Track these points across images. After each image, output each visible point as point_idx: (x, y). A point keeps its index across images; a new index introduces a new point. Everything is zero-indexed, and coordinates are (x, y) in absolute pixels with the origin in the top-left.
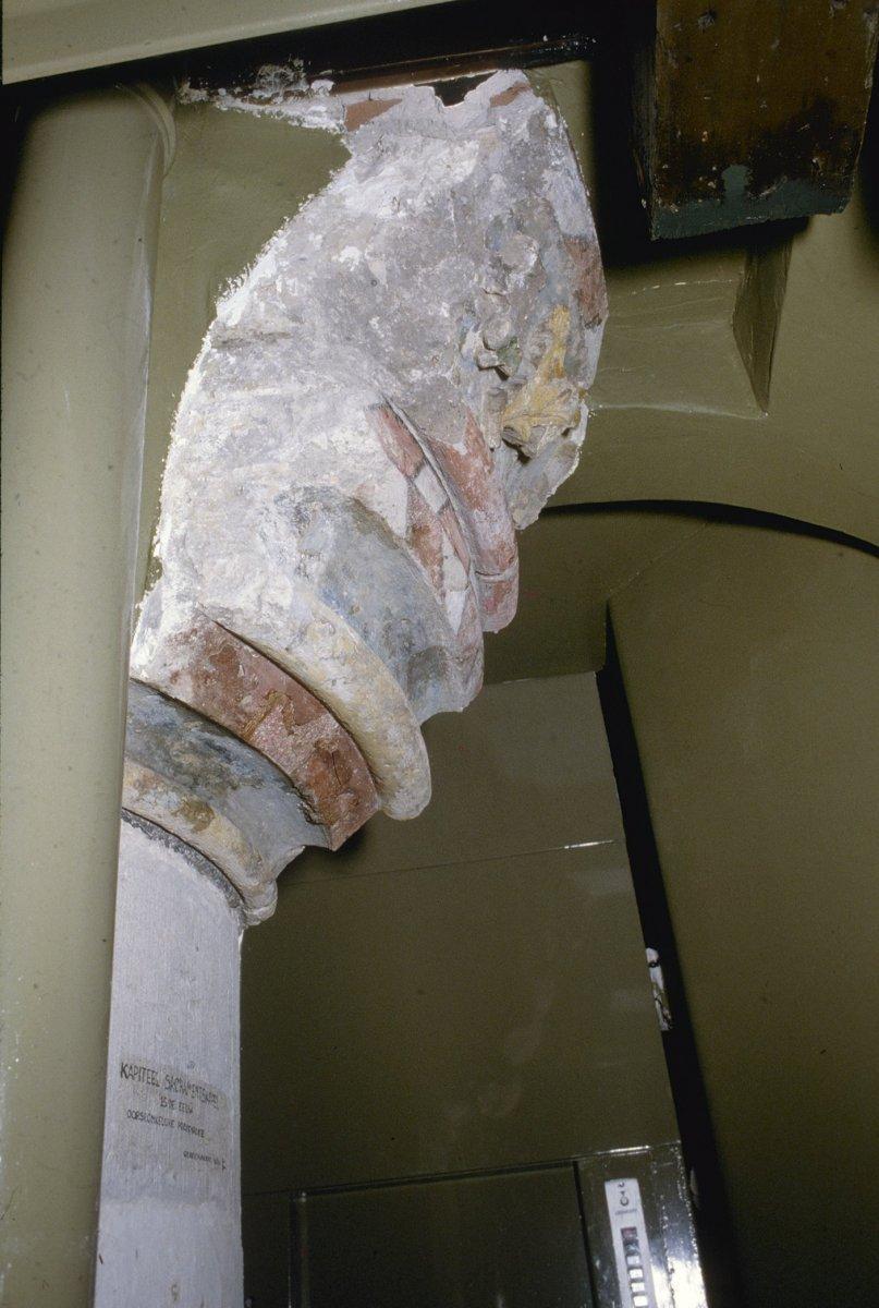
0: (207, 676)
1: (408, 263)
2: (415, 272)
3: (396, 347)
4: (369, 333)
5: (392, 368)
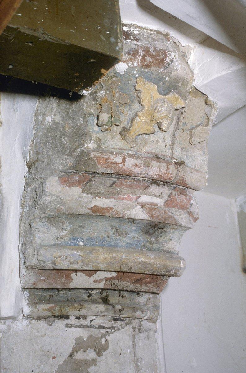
0: (44, 280)
1: (66, 111)
2: (68, 113)
3: (71, 144)
4: (62, 144)
5: (70, 154)
